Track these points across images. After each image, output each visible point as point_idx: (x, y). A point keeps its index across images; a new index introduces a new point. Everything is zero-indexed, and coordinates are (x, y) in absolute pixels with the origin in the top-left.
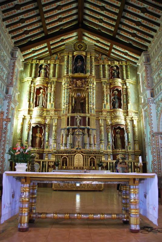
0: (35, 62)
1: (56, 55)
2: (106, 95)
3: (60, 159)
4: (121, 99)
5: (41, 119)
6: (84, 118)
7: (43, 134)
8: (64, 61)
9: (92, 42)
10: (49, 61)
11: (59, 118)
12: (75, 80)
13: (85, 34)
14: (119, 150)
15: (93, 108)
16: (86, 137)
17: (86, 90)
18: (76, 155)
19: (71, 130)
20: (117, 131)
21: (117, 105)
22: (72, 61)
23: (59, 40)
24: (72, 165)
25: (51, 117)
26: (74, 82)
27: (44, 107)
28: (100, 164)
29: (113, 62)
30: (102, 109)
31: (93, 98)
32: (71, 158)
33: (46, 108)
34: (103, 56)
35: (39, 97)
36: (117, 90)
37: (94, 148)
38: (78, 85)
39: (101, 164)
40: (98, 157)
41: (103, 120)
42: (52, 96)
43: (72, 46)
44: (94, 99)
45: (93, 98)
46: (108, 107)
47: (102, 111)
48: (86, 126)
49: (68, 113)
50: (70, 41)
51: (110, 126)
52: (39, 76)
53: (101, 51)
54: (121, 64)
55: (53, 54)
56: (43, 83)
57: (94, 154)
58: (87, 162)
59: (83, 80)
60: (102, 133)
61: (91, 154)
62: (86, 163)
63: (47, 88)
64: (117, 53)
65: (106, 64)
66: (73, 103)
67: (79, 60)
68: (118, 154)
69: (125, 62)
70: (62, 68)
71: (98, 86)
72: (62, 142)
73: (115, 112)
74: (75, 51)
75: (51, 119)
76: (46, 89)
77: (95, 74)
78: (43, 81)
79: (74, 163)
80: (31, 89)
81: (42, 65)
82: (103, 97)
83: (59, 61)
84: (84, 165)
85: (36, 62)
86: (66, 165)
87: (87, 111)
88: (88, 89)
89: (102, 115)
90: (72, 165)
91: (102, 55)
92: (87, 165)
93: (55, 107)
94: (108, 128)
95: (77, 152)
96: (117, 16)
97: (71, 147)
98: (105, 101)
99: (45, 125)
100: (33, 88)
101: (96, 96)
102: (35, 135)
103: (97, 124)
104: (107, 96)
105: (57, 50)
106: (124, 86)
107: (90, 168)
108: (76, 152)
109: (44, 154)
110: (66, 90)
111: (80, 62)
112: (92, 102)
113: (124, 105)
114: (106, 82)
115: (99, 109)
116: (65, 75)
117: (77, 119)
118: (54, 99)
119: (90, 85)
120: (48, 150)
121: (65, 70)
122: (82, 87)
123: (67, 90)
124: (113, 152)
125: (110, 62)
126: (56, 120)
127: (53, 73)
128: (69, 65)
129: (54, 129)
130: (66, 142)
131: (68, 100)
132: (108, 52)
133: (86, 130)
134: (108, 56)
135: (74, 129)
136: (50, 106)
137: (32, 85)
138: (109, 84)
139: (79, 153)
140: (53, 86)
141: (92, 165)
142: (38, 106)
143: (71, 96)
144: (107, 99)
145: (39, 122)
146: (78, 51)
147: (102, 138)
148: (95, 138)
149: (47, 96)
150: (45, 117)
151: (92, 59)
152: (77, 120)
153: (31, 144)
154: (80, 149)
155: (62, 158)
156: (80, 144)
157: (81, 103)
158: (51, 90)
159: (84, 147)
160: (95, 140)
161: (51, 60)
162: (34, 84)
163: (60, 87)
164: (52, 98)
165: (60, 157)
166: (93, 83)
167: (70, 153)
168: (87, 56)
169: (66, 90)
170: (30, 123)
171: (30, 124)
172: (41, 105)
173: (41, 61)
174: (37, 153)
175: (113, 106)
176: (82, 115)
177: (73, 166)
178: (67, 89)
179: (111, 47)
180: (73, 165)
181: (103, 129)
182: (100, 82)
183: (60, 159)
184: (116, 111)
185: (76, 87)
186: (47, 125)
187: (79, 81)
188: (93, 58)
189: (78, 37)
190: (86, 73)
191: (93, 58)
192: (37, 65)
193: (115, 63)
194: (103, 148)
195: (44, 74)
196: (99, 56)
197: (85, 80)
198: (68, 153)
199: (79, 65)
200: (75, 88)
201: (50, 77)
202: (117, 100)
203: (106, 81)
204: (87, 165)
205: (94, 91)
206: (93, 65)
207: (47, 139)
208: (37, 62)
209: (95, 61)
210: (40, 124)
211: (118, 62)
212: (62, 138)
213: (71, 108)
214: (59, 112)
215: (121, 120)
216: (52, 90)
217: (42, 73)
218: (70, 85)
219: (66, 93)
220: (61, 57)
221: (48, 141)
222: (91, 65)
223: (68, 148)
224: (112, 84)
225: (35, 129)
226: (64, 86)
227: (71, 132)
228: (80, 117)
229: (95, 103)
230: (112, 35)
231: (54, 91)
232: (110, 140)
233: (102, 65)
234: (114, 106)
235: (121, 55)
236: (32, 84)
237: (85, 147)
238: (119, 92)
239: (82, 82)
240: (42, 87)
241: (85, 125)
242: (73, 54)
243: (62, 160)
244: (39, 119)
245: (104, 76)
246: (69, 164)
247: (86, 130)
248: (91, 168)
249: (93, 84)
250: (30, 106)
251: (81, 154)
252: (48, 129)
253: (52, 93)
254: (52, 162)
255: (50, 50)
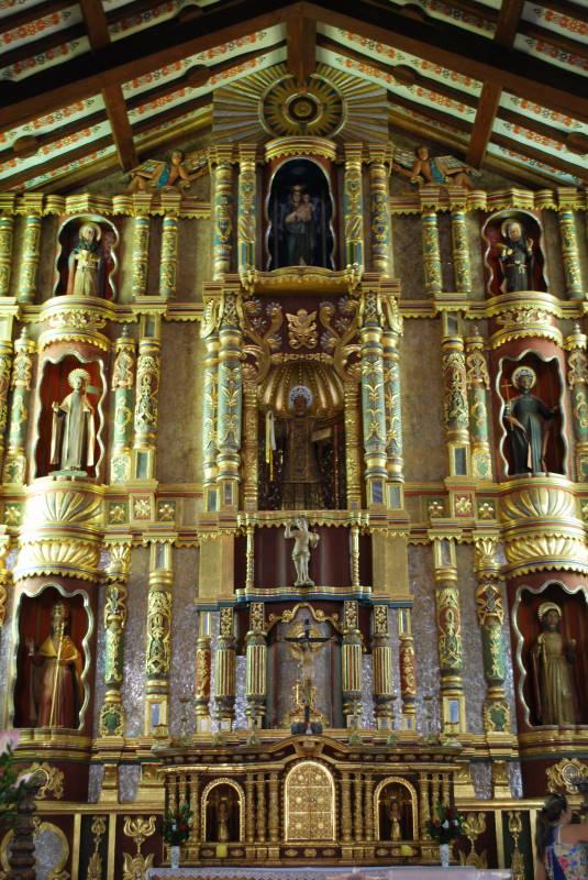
0: (37, 206)
1: (163, 164)
2: (464, 391)
3: (194, 795)
4: (558, 416)
5: (71, 551)
6: (339, 536)
7: (85, 643)
8: (205, 197)
9: (373, 79)
10: (116, 200)
11: (185, 543)
12: (275, 309)
13: (327, 35)
14: (561, 730)
15: (391, 474)
16: (352, 653)
17: (347, 366)
18: (294, 769)
19: (257, 612)
20: (543, 610)
21: (535, 451)
22: (254, 193)
23: (174, 73)
24: (267, 836)
25: (136, 534)
26: (269, 325)
27: (93, 474)
28: (446, 825)
29: (501, 193)
30: (448, 480)
31: (389, 412)
32: (261, 788)
33: (105, 479)
34: (440, 159)
35: (62, 414)
36: (533, 360)
37: (404, 725)
38: (298, 334)
39: (451, 825)
40: (430, 777)
41: (452, 545)
42: (141, 410)
43: (254, 109)
44: (397, 417)
45: (389, 412)
46: (482, 465)
47: (446, 493)
48: (350, 584)
49: (241, 508)
50: (239, 76)
51: (496, 580)
52: (62, 290)
53: (430, 133)
54: (550, 204)
55: (144, 157)
56: (82, 331)
57: (402, 758)
58: (363, 815)
59: (328, 309)
60: (451, 626)
61: (388, 758)
62: (358, 823)
63: (109, 358)
64: (522, 137)
65: (459, 208)
66: (270, 444)
67: (297, 188)
68: (556, 759)
69: (574, 191)
70: (195, 240)
71: (415, 341)
72: (207, 689)
74: (271, 138)
75: (138, 547)
76: (101, 363)
77: (395, 267)
78: (86, 316)
79: (281, 824)
80: (12, 369)
81: (75, 226)
82: (452, 408)
83: (178, 197)
84: (348, 831)
85: (44, 207)
86: (233, 836)
87: (352, 495)
88: (354, 358)
89: (445, 513)
90: (267, 836)
91: (433, 155)
92: (364, 835)
93: (158, 472)
94: (484, 596)
95: (297, 748)
96: (482, 80)
97: (264, 718)
98: (464, 432)
99: (97, 586)
100: (22, 361)
101: (406, 398)
102: (37, 649)
103: (420, 569)
104: (472, 400)
105: (167, 132)
106: (572, 333)
107: (382, 852)
108: (289, 750)
109: (94, 770)
110: (222, 367)
111: (302, 202)
112: (383, 436)
113: (576, 449)
114: (463, 313)
115: (426, 478)
116: (216, 277)
117: (291, 542)
118: (150, 423)
119: (366, 337)
120: (116, 740)
121: (218, 250)
122: (319, 349)
123: (231, 367)
124: (522, 747)
125: (483, 195)
126: (167, 551)
127: (142, 268)
128: (241, 219)
129: (152, 610)
130: (231, 687)
131: (237, 433)
132: (468, 138)
133: (351, 610)
134: (472, 157)
135: (275, 606)
136: (128, 466)
137: (20, 344)
138: (485, 323)
139: (309, 755)
140: (143, 349)
141: (397, 831)
142: (58, 467)
143: (252, 404)
145: (62, 566)
146: (291, 134)
147: (453, 659)
148: (407, 659)
149: (109, 406)
150: (100, 536)
151: (377, 179)
152: (296, 551)
153: (11, 708)
154: (317, 730)
155: (206, 794)
156: (318, 698)
157: (316, 445)
158: (133, 371)
159: (345, 716)
160: (408, 670)
161: (129, 194)
162: (31, 337)
163: (189, 351)
164: (138, 417)
165: (194, 782)
166: (387, 322)
167: (257, 759)
168: (343, 165)
169: (222, 367)
170: (10, 577)
172: (71, 460)
173: (69, 200)
174: (52, 762)
175: (515, 457)
176: (326, 517)
177: (274, 839)
178: (231, 363)
179: (487, 108)
180: (274, 832)
181: (455, 603)
182: (428, 318)
183: (194, 795)
184: (531, 491)
185: (285, 347)
186: (110, 582)
187: (302, 312)
188: (382, 172)
189: (290, 53)
190: (340, 267)
191: (382, 172)
192: (46, 222)
193: (517, 202)
194: (458, 720)
195: (89, 277)
196: (415, 163)
197: (336, 308)
198: (245, 760)
199: (300, 216)
200: (276, 357)
201: (124, 293)
202: (535, 423)
203: (465, 309)
204: (364, 835)
205: (396, 373)
206: (381, 218)
207: (109, 672)
208: (50, 208)
209: (393, 191)
210: (70, 581)
211: (530, 195)
212: (202, 663)
213: (253, 476)
214: (181, 501)
215: (562, 541)
216: (141, 371)
217: (80, 275)
218: (247, 340)
219: (222, 389)
220: (190, 173)
221: (117, 685)
222: (372, 216)
223: (245, 720)
224: (502, 327)
226: (210, 347)
227: (257, 627)
228: (311, 529)
229: (400, 446)
230: (490, 35)
231: (153, 378)
232: (503, 667)
233: (439, 213)
234: (519, 465)
235: (551, 148)
236: (15, 335)
237: (349, 718)
238: (547, 371)
239: (317, 320)
240: (77, 354)
241: (342, 578)
242: (261, 152)
243: (205, 803)
244: (63, 548)
245: (452, 281)
246: (251, 826)
247: (351, 610)
248: (389, 849)
249: (388, 327)
251: (324, 762)
252: (120, 608)
253: (142, 392)
254: (146, 818)
255: (123, 134)
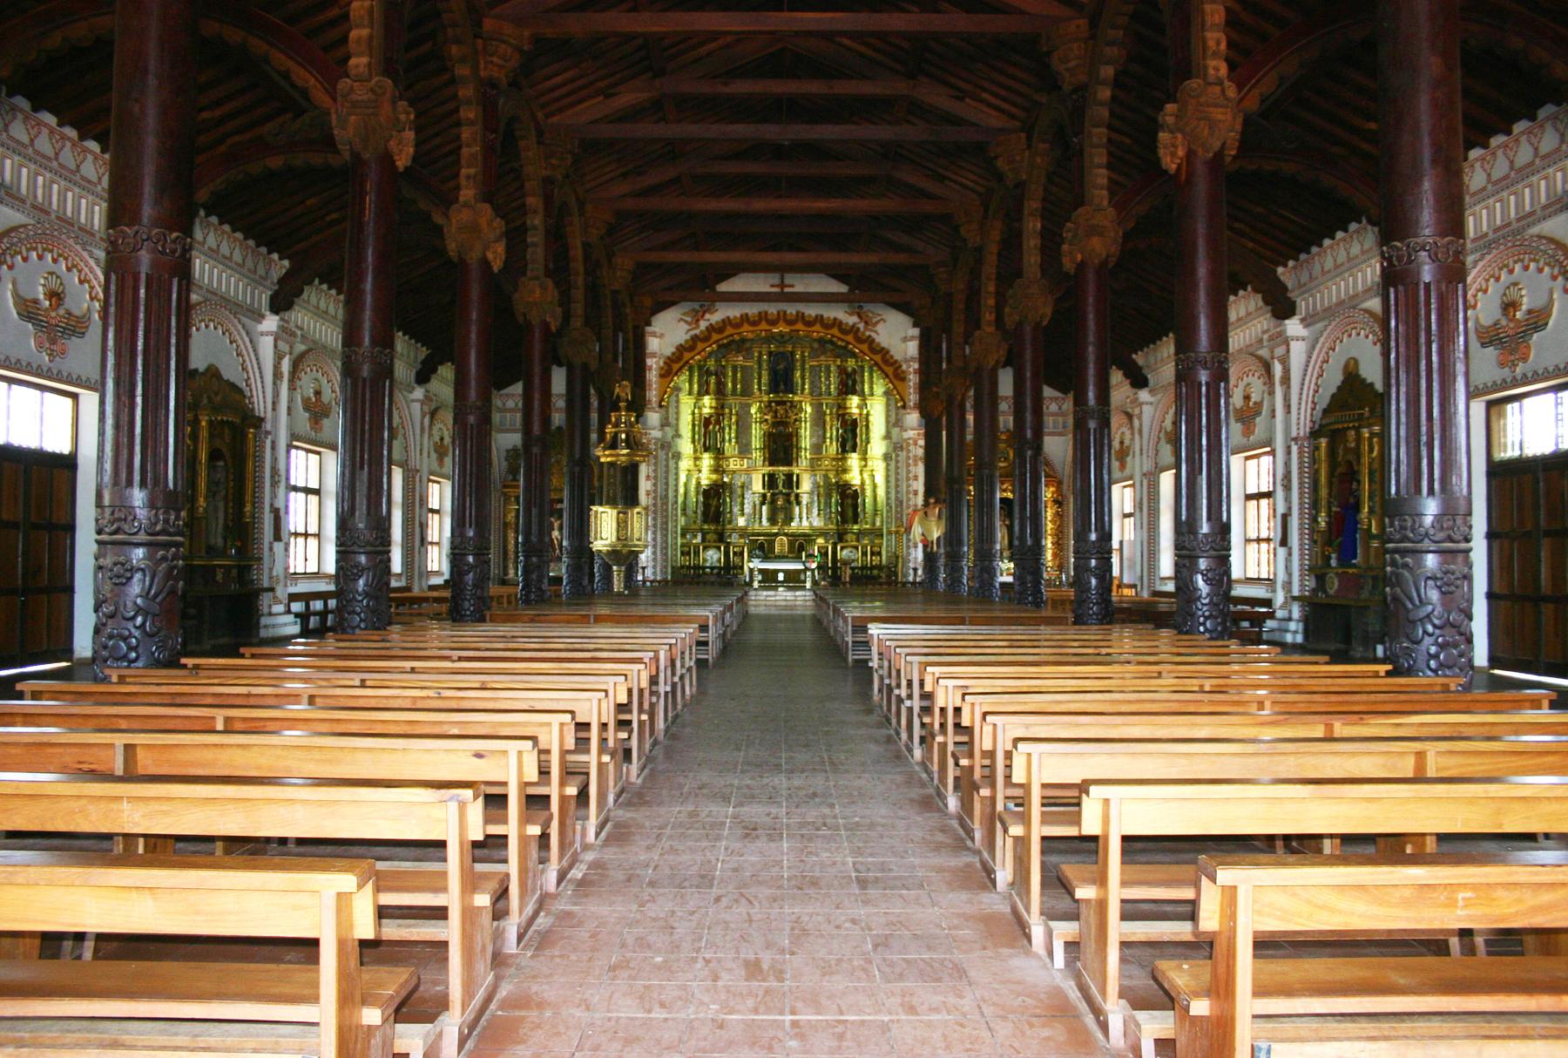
46: (832, 448)
73: (844, 459)
144: (833, 430)
171: (698, 484)
225: (707, 493)
234: (844, 451)
250: (695, 451)
